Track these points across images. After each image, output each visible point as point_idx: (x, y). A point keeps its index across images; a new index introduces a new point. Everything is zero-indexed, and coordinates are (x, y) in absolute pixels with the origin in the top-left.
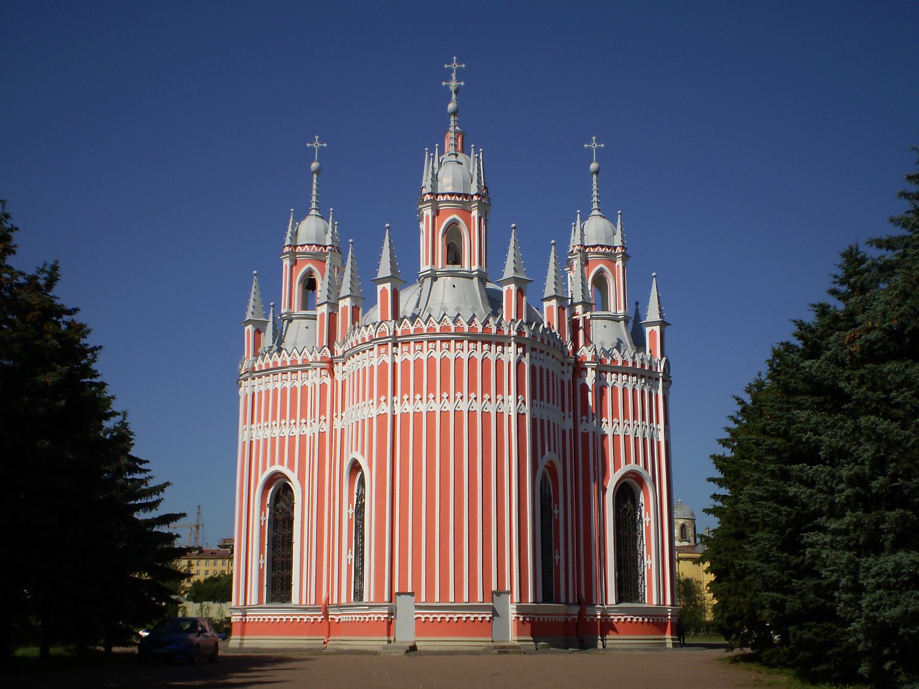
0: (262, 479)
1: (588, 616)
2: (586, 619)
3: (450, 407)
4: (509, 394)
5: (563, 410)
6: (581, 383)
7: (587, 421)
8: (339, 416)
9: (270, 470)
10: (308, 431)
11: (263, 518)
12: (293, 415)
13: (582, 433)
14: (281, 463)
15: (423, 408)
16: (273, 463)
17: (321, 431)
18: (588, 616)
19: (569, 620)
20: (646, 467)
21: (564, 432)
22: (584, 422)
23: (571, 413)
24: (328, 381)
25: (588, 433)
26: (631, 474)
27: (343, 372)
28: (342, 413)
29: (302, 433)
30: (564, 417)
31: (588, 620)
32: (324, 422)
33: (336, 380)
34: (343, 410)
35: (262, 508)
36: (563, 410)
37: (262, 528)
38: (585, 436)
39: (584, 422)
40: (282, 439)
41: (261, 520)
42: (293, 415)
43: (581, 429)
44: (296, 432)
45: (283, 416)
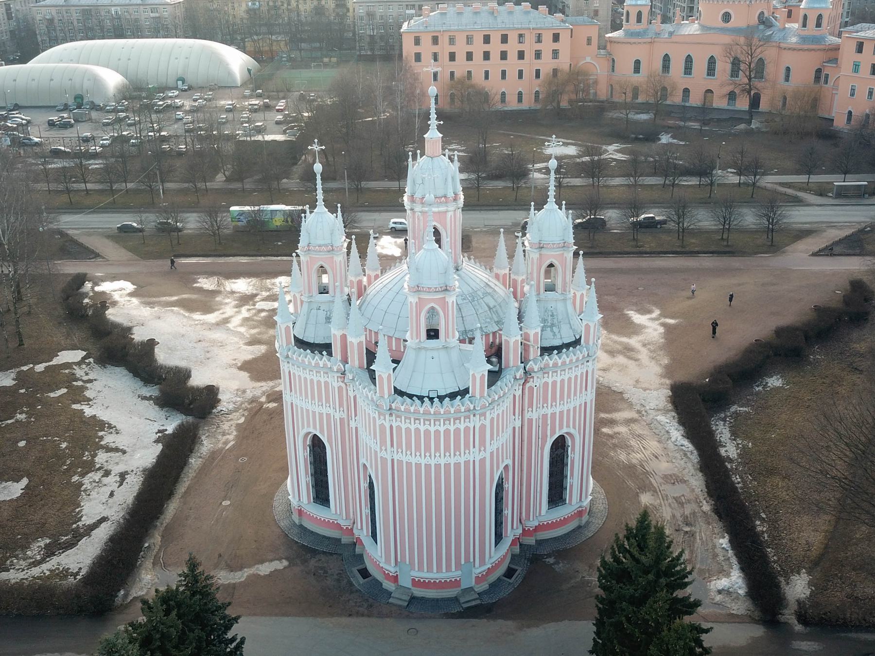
0: (302, 433)
3: (433, 462)
4: (474, 447)
7: (532, 411)
8: (354, 420)
11: (305, 454)
13: (528, 419)
15: (414, 460)
20: (574, 427)
21: (514, 428)
22: (530, 412)
23: (520, 417)
24: (343, 385)
25: (532, 419)
30: (515, 419)
34: (356, 416)
35: (305, 449)
36: (514, 414)
37: (305, 460)
39: (530, 412)
43: (527, 416)
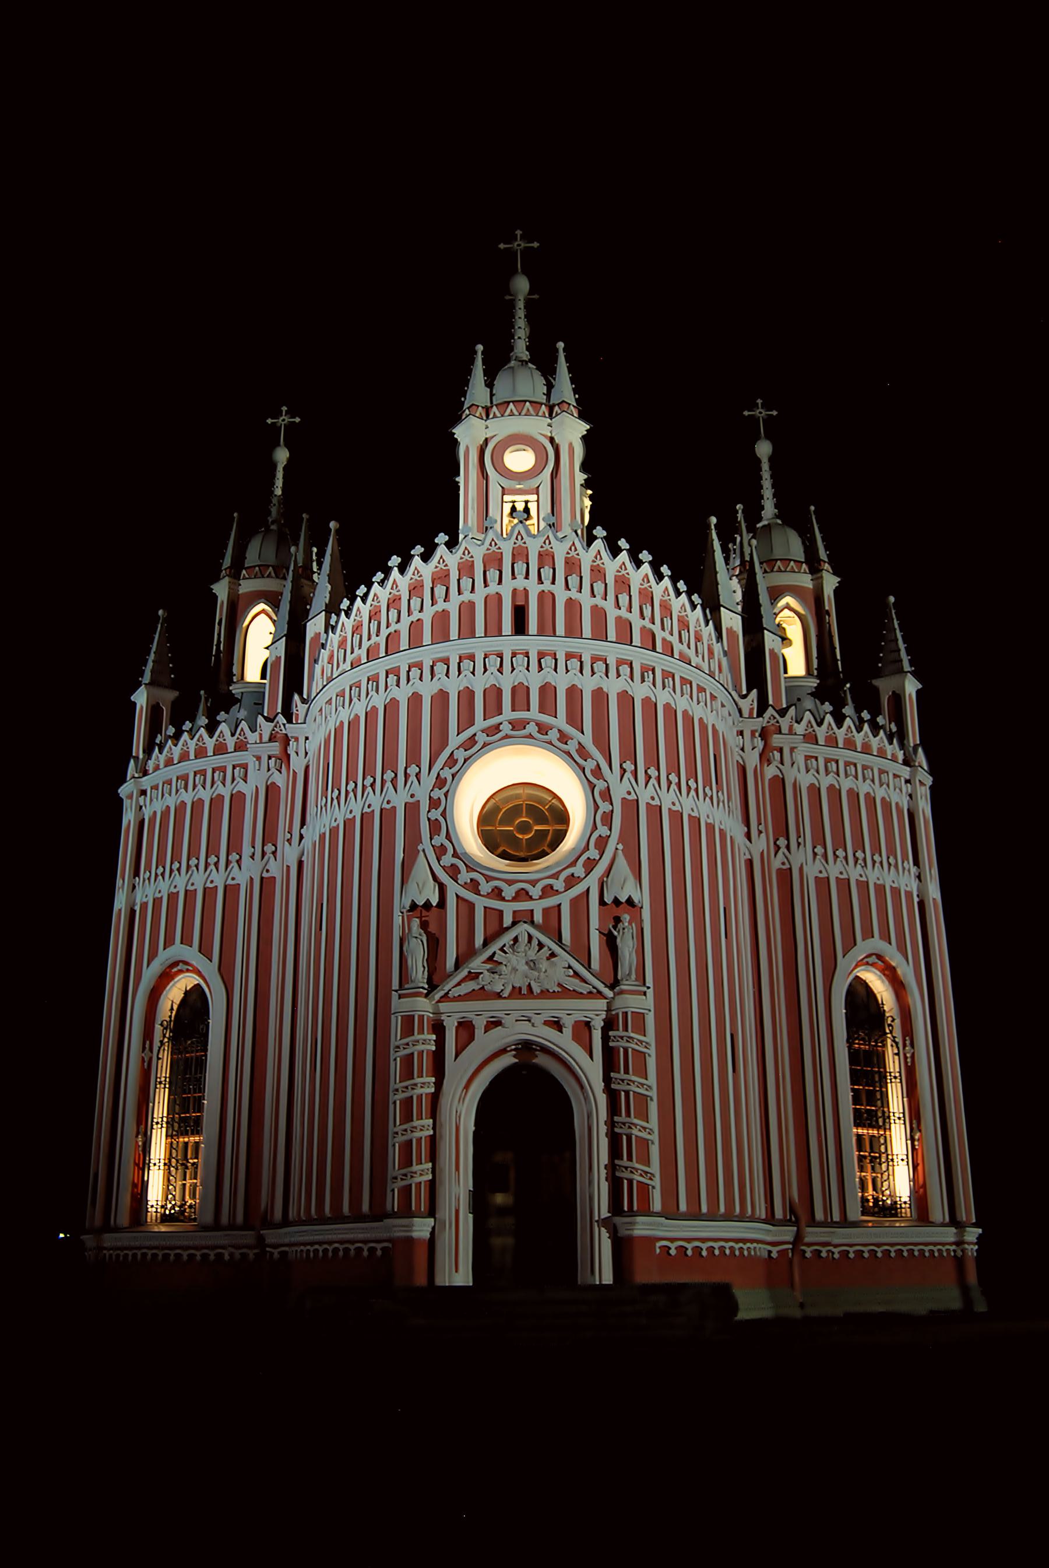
1: (809, 1245)
2: (804, 1252)
5: (747, 822)
6: (770, 777)
7: (788, 847)
9: (164, 956)
10: (241, 877)
12: (212, 848)
13: (779, 871)
14: (186, 940)
16: (169, 942)
17: (265, 875)
18: (809, 1245)
19: (774, 1255)
21: (750, 863)
22: (783, 850)
23: (761, 827)
26: (874, 957)
27: (306, 753)
28: (302, 827)
29: (230, 882)
31: (808, 1255)
32: (271, 855)
33: (295, 772)
34: (303, 823)
36: (747, 822)
38: (785, 876)
39: (783, 850)
40: (190, 895)
41: (143, 1058)
42: (212, 848)
44: (219, 879)
45: (193, 852)
